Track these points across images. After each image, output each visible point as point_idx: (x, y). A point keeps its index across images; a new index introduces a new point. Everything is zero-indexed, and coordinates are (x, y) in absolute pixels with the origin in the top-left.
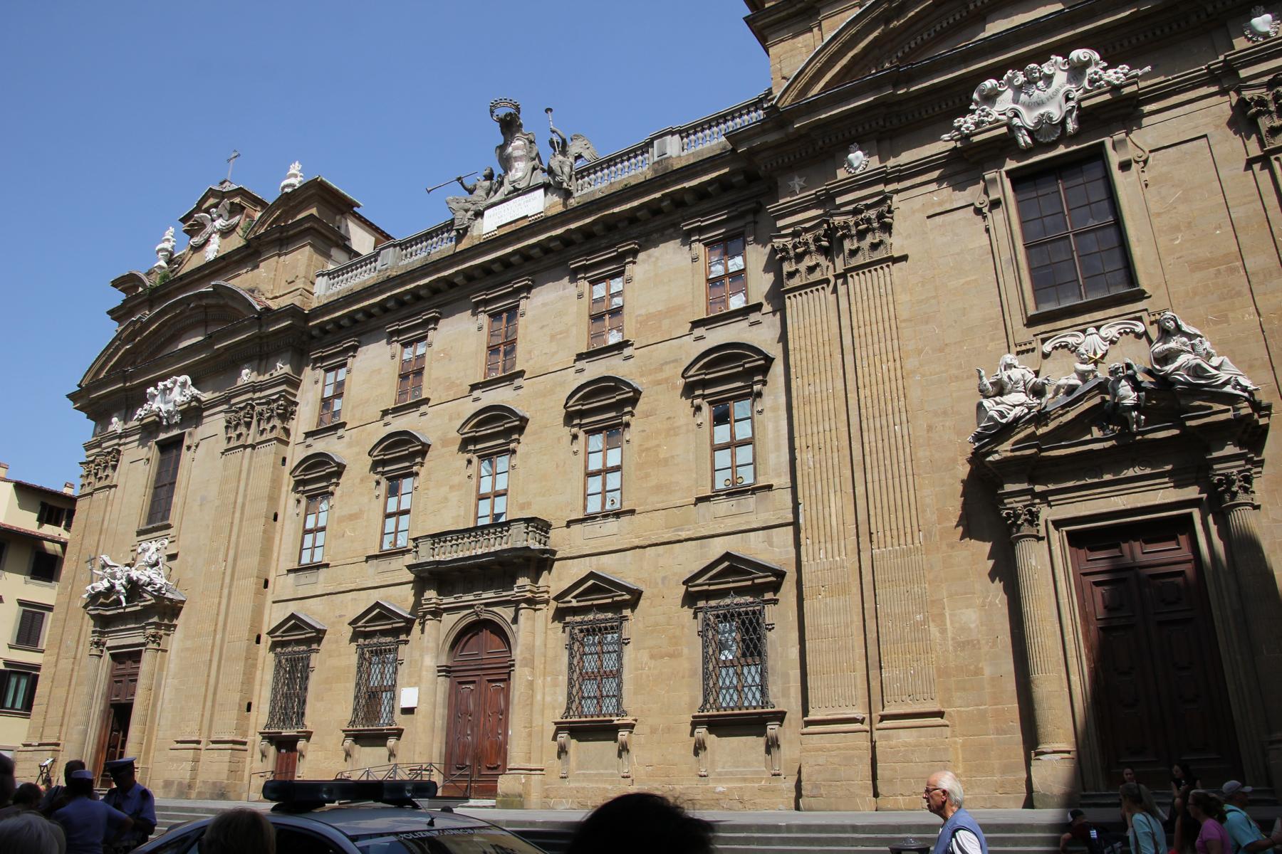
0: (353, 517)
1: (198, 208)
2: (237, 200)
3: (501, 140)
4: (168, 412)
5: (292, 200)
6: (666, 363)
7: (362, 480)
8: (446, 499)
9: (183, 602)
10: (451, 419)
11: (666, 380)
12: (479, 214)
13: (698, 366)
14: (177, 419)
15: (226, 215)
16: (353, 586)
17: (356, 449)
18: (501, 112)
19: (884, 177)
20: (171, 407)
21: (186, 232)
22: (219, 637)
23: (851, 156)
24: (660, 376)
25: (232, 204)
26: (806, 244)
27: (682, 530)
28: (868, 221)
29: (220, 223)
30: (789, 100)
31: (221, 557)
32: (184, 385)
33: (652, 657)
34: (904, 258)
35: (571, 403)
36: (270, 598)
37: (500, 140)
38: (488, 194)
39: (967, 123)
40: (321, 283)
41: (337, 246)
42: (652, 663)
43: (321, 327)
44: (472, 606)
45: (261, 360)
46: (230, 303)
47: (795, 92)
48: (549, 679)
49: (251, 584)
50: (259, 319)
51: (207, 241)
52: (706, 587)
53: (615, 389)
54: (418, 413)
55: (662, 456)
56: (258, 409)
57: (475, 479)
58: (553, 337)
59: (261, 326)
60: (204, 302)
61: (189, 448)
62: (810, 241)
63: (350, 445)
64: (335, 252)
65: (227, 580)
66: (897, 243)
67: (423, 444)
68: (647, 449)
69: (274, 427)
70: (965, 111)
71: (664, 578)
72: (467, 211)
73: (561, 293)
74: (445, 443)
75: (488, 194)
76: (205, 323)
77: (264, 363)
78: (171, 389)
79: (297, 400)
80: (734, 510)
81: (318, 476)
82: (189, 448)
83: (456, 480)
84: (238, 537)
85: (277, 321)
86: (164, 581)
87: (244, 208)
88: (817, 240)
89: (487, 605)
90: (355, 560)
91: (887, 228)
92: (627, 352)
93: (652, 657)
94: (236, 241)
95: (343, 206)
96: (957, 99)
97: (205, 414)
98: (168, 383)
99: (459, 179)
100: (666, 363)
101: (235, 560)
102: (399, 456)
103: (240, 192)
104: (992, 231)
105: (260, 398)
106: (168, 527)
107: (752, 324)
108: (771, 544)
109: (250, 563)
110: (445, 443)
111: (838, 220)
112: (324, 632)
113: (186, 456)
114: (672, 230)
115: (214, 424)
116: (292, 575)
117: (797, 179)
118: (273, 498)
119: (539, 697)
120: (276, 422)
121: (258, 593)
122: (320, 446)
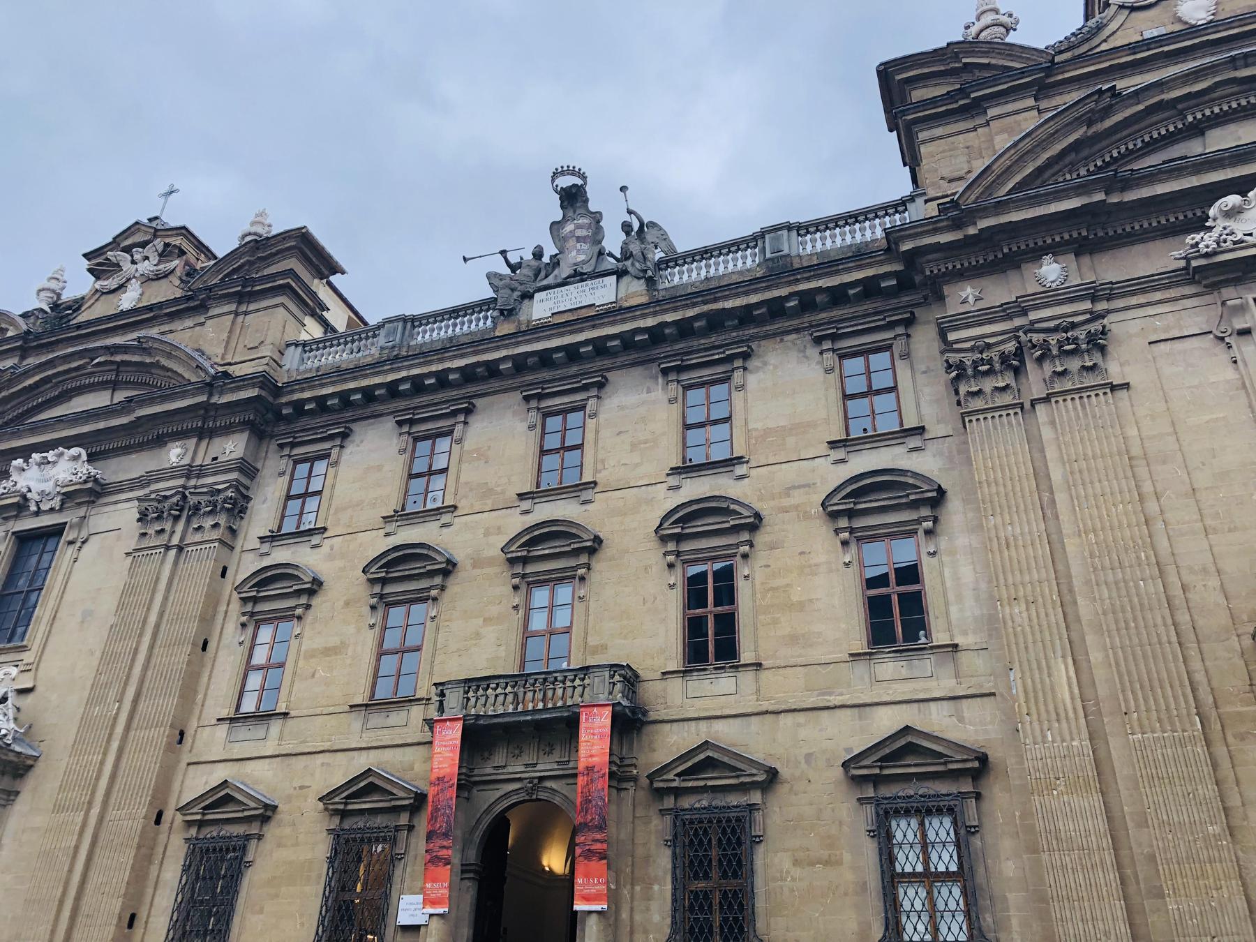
0: (328, 652)
1: (115, 243)
2: (176, 241)
3: (558, 215)
4: (42, 494)
5: (259, 248)
6: (794, 487)
7: (347, 604)
8: (478, 635)
9: (36, 758)
10: (487, 534)
11: (796, 507)
12: (528, 296)
13: (843, 493)
14: (56, 503)
15: (154, 259)
16: (326, 746)
17: (339, 563)
18: (566, 181)
19: (1093, 293)
20: (48, 487)
21: (90, 270)
22: (95, 811)
23: (1044, 268)
24: (786, 502)
25: (167, 245)
26: (990, 362)
27: (830, 694)
28: (1075, 340)
29: (146, 267)
30: (973, 197)
31: (112, 695)
32: (75, 458)
33: (796, 863)
34: (1126, 386)
35: (666, 525)
36: (186, 758)
37: (558, 215)
38: (536, 276)
39: (1207, 241)
40: (293, 355)
41: (313, 314)
42: (797, 872)
43: (298, 406)
44: (520, 779)
45: (200, 439)
46: (164, 362)
47: (980, 189)
48: (638, 888)
49: (161, 735)
50: (210, 385)
51: (121, 287)
52: (877, 771)
53: (726, 512)
54: (438, 524)
55: (795, 598)
56: (192, 500)
57: (521, 612)
58: (634, 446)
59: (211, 395)
60: (118, 358)
61: (71, 543)
62: (996, 359)
63: (331, 557)
64: (308, 320)
65: (119, 729)
66: (1115, 371)
67: (449, 561)
68: (773, 589)
69: (216, 526)
70: (1200, 224)
71: (808, 757)
72: (513, 290)
73: (645, 395)
74: (477, 563)
75: (536, 276)
76: (114, 386)
77: (204, 443)
78: (55, 463)
79: (250, 494)
80: (904, 673)
81: (279, 594)
82: (71, 543)
83: (494, 610)
84: (146, 668)
85: (239, 389)
86: (12, 725)
87: (182, 253)
88: (1004, 358)
89: (541, 779)
90: (331, 709)
91: (1102, 349)
92: (740, 470)
93: (796, 863)
94: (168, 291)
95: (326, 266)
96: (1189, 212)
97: (106, 500)
98: (51, 455)
99: (503, 253)
100: (794, 487)
101: (136, 701)
102: (408, 575)
103: (183, 231)
104: (1239, 362)
105: (196, 487)
106: (24, 649)
107: (911, 450)
108: (961, 720)
109: (160, 706)
110: (477, 563)
111: (1036, 337)
112: (274, 808)
113: (65, 555)
114: (794, 336)
115: (121, 516)
116: (225, 727)
117: (969, 290)
118: (207, 619)
119: (625, 915)
120: (222, 519)
121: (169, 749)
122: (281, 555)
